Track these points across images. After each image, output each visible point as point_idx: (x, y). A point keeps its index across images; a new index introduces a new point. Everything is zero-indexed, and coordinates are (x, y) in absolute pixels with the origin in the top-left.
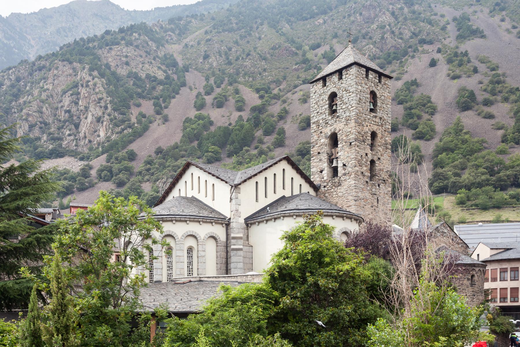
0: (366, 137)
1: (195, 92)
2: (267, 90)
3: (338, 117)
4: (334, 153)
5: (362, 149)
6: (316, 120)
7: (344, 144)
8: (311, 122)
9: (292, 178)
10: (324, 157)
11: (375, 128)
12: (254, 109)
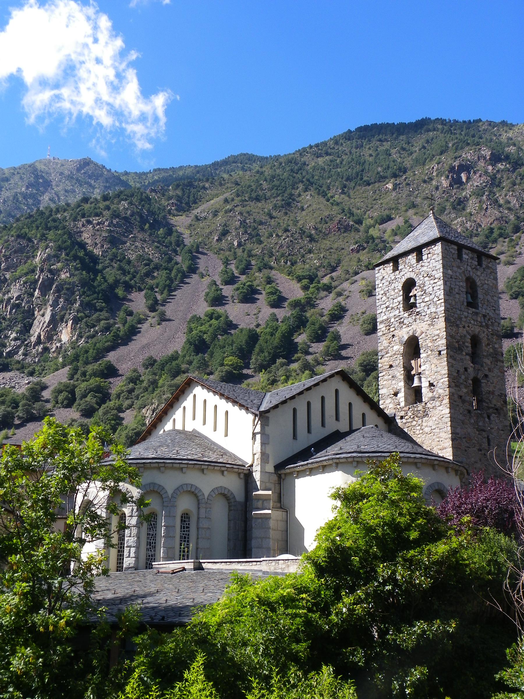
0: (464, 343)
1: (206, 280)
3: (418, 313)
4: (413, 365)
6: (385, 317)
7: (430, 352)
8: (378, 320)
9: (350, 404)
10: (399, 372)
11: (477, 330)
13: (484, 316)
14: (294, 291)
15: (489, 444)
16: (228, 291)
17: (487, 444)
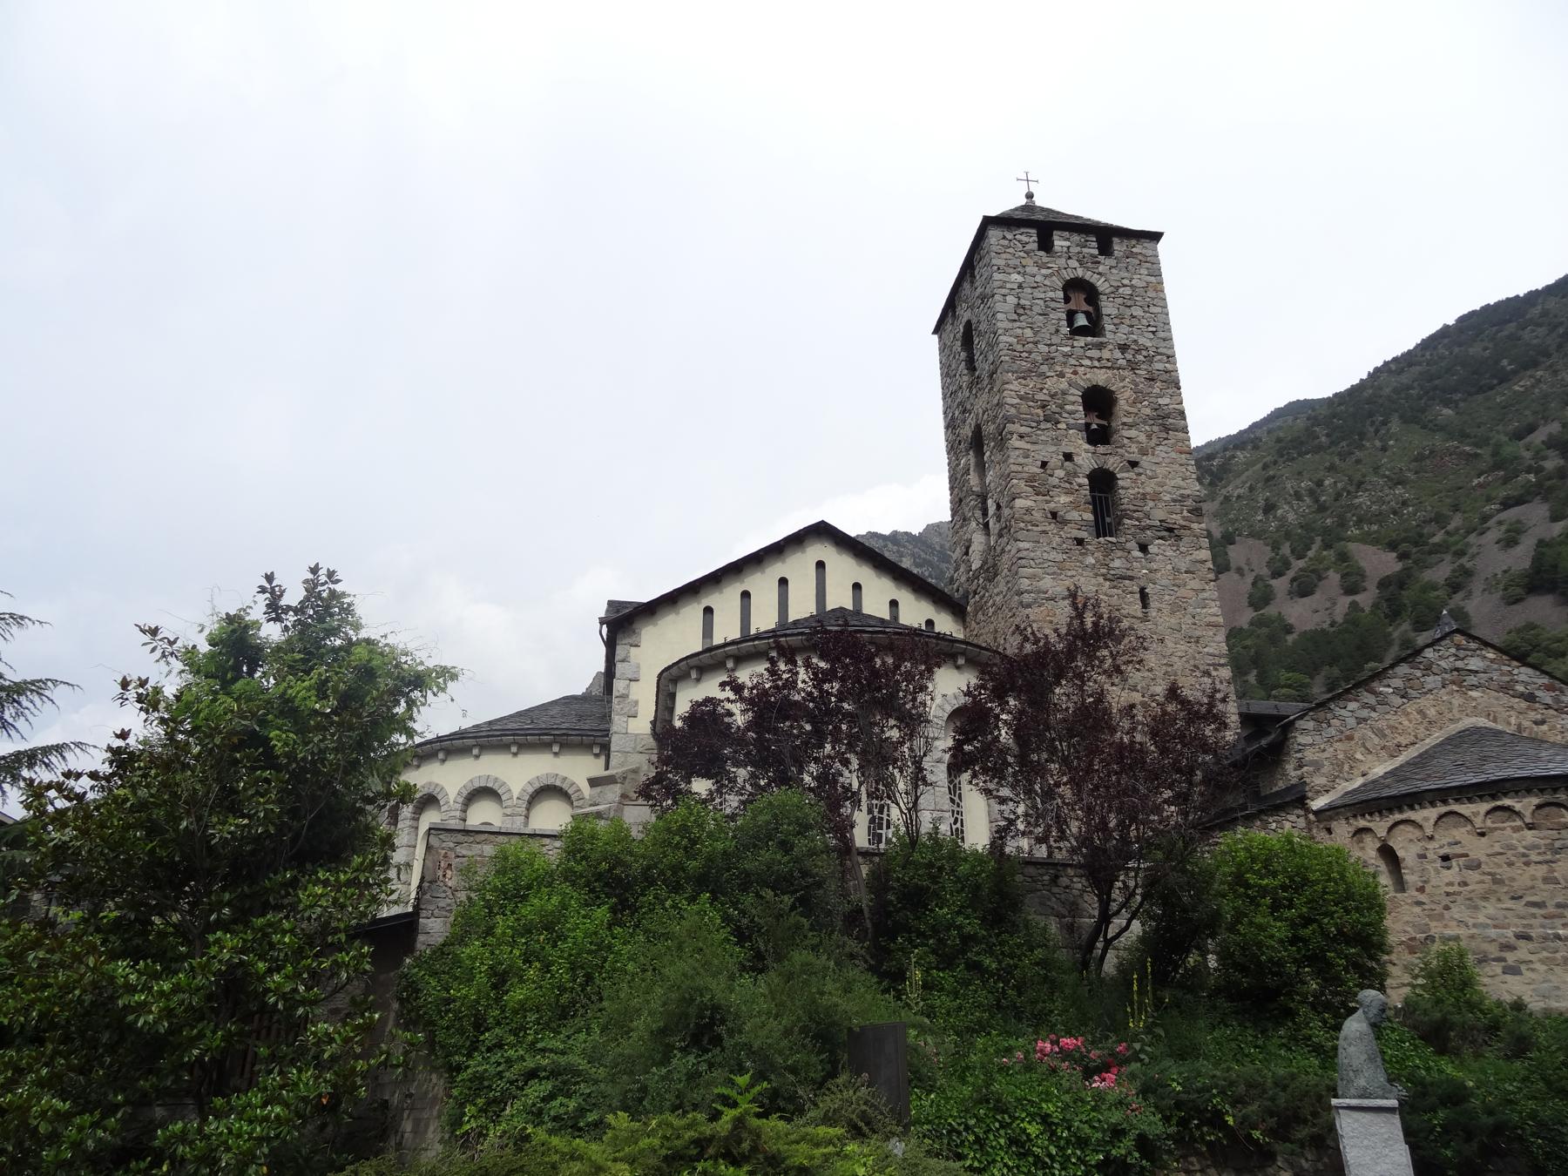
1: (1250, 579)
2: (1419, 540)
9: (857, 587)
11: (1101, 378)
12: (1384, 584)
13: (1123, 348)
14: (1379, 563)
15: (1145, 605)
16: (1280, 585)
17: (1139, 606)
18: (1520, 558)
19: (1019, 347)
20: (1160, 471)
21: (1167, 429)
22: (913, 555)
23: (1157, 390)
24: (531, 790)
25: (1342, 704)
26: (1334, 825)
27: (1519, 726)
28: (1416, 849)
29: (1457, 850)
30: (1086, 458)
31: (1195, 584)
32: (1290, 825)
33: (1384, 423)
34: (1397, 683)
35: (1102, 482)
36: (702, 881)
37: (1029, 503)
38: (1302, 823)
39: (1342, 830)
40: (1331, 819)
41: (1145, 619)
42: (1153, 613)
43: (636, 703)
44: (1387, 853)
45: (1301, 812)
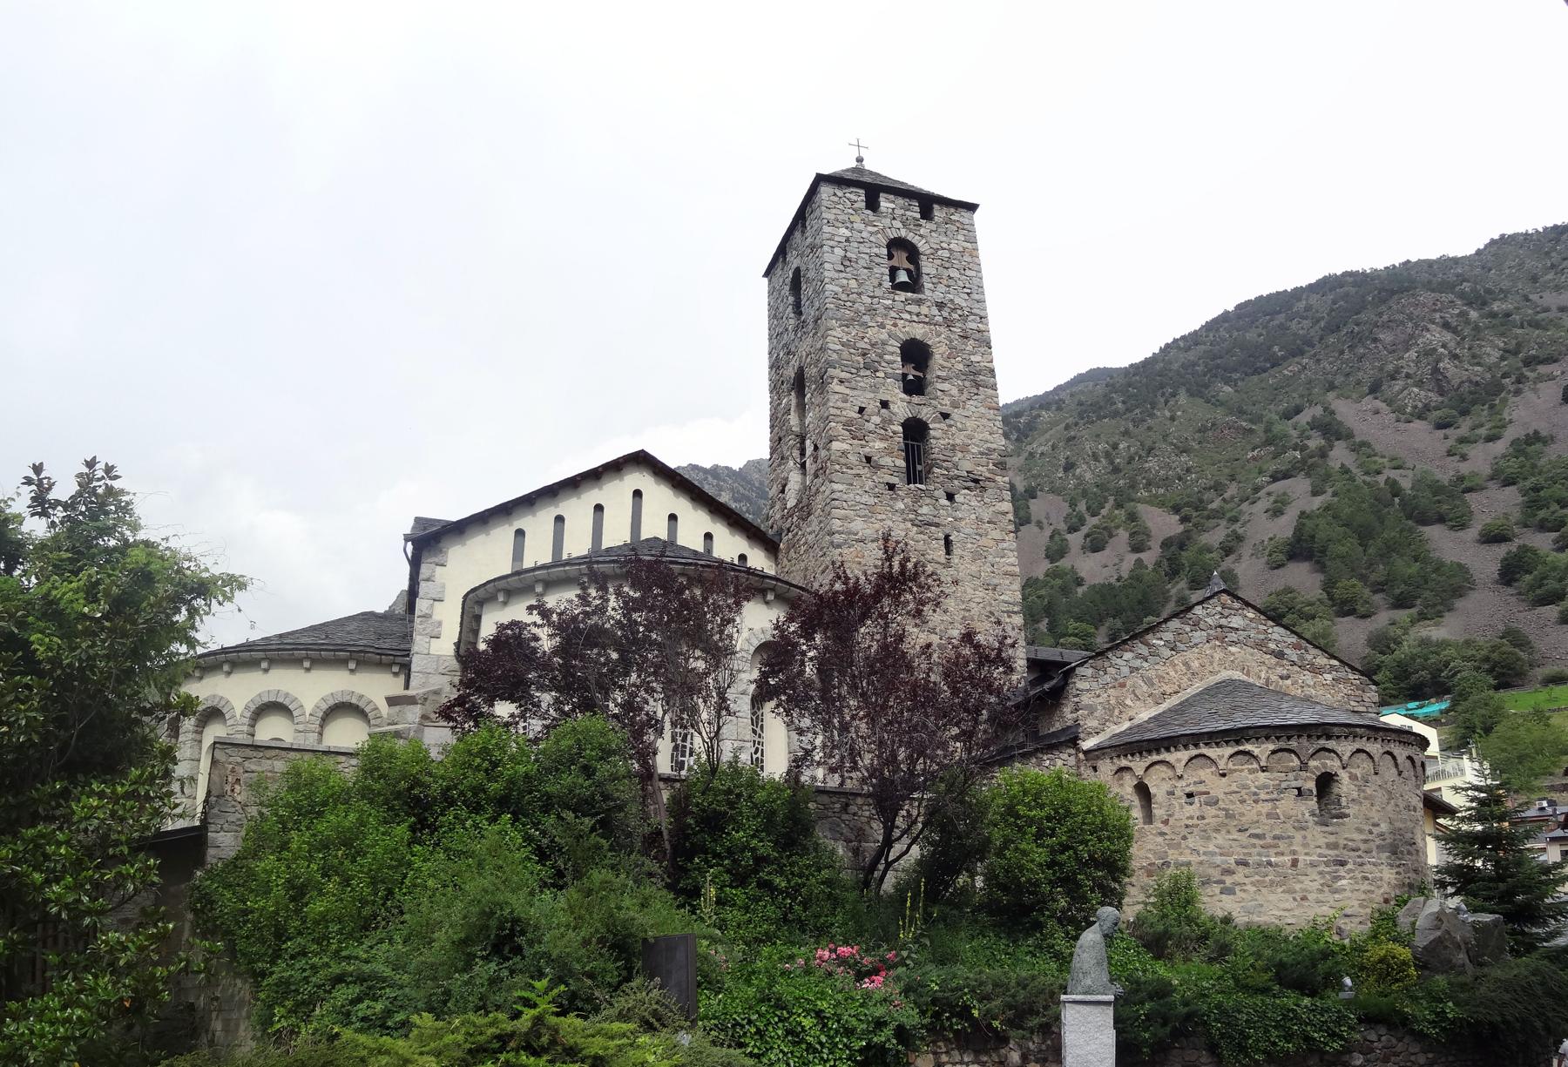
1: (1048, 533)
2: (1199, 505)
5: (864, 389)
9: (673, 518)
11: (918, 332)
12: (1166, 544)
13: (940, 306)
14: (1163, 524)
16: (1075, 540)
17: (943, 552)
18: (1284, 528)
19: (844, 297)
20: (970, 424)
21: (978, 386)
22: (732, 490)
23: (969, 348)
24: (325, 707)
25: (1119, 653)
26: (1100, 764)
27: (1268, 679)
28: (1166, 787)
29: (1202, 788)
30: (902, 407)
31: (996, 534)
32: (1062, 763)
33: (1174, 395)
34: (1169, 636)
35: (915, 431)
36: (503, 803)
37: (845, 446)
38: (1072, 761)
39: (1106, 767)
40: (1098, 758)
41: (948, 565)
42: (955, 560)
43: (440, 624)
44: (1143, 790)
45: (1072, 751)
